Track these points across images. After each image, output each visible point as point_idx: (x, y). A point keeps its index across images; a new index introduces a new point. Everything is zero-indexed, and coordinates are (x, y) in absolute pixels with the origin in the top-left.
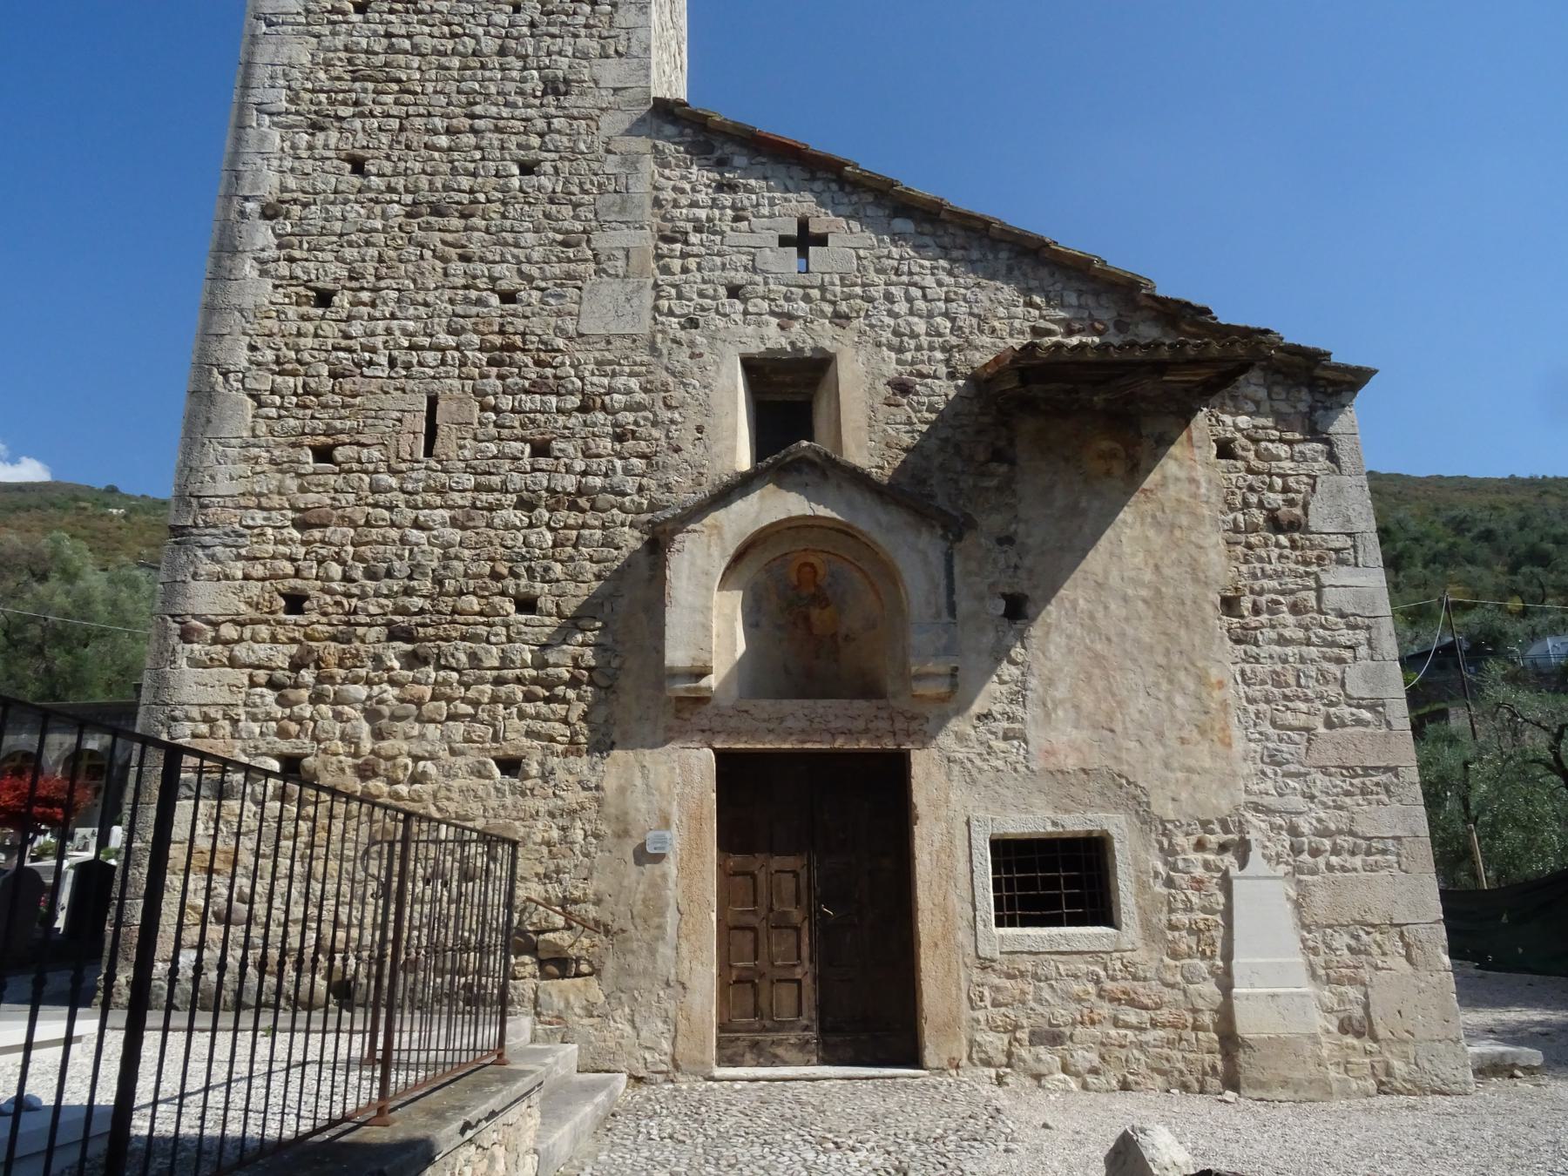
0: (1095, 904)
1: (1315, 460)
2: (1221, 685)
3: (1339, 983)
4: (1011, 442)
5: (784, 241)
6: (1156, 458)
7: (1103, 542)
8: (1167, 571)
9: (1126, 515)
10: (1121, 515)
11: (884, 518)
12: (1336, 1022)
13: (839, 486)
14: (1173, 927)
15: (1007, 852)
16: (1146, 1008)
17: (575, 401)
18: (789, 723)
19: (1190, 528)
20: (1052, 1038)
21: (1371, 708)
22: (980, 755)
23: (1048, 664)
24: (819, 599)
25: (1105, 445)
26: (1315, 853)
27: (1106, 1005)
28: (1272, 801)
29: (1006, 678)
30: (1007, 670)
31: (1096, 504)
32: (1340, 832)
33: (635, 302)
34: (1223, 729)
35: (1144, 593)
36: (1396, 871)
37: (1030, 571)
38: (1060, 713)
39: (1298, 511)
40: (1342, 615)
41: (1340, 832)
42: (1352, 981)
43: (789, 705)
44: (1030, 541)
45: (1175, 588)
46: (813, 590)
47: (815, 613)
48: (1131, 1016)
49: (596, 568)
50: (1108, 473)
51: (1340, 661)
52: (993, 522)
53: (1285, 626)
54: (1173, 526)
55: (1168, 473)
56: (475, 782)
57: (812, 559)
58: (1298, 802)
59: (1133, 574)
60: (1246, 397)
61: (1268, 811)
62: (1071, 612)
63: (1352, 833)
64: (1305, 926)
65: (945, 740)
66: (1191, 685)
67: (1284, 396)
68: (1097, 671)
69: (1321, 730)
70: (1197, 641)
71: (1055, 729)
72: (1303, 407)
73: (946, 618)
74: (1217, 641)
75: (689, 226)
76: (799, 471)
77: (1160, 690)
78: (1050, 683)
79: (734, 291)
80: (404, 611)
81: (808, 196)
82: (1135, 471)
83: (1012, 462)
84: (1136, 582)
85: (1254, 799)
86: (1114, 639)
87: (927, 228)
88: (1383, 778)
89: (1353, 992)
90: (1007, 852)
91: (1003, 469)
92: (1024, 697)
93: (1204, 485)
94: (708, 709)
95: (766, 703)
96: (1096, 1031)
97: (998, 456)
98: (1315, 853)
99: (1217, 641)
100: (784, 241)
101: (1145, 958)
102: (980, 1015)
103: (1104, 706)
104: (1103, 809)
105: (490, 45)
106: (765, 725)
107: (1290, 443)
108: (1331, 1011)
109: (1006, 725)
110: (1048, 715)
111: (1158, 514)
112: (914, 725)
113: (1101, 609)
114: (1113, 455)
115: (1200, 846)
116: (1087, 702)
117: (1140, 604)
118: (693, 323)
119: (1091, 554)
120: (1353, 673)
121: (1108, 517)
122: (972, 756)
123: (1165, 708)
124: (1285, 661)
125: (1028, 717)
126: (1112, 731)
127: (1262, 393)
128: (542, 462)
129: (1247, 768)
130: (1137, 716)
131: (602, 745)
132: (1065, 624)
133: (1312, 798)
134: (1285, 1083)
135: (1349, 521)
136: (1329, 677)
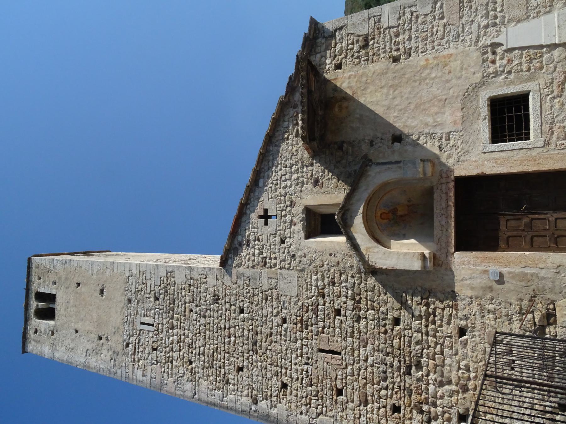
0: (520, 101)
2: (427, 60)
4: (336, 143)
5: (266, 224)
6: (341, 91)
7: (372, 108)
8: (383, 84)
9: (362, 100)
10: (362, 102)
11: (364, 188)
13: (352, 204)
14: (529, 70)
15: (496, 137)
17: (320, 299)
18: (443, 223)
19: (367, 76)
22: (456, 149)
23: (419, 125)
24: (394, 211)
25: (337, 109)
26: (496, 17)
28: (474, 36)
29: (425, 141)
30: (422, 141)
31: (358, 111)
32: (487, 9)
33: (286, 276)
34: (445, 58)
35: (391, 92)
37: (383, 134)
38: (439, 120)
39: (361, 38)
40: (400, 18)
41: (487, 9)
43: (436, 223)
44: (372, 134)
45: (389, 80)
46: (390, 214)
47: (399, 213)
49: (382, 295)
50: (347, 108)
51: (417, 17)
52: (365, 148)
53: (404, 38)
54: (366, 83)
55: (347, 86)
56: (469, 346)
57: (379, 215)
58: (474, 26)
59: (384, 96)
60: (320, 61)
61: (478, 37)
62: (399, 118)
63: (487, 4)
64: (528, 18)
65: (450, 163)
66: (428, 71)
67: (319, 48)
68: (422, 107)
69: (445, 21)
70: (409, 70)
71: (445, 121)
72: (323, 41)
73: (401, 165)
74: (410, 63)
75: (261, 256)
76: (346, 219)
77: (429, 83)
78: (427, 124)
79: (283, 241)
80: (399, 368)
81: (251, 215)
82: (345, 98)
83: (343, 142)
84: (387, 95)
86: (409, 101)
87: (262, 175)
90: (496, 137)
91: (345, 145)
92: (432, 134)
93: (351, 73)
94: (438, 254)
95: (435, 232)
97: (340, 148)
98: (496, 17)
99: (410, 63)
100: (266, 224)
103: (436, 103)
104: (478, 101)
105: (203, 321)
106: (444, 232)
107: (336, 44)
110: (439, 124)
111: (362, 88)
112: (444, 175)
113: (397, 107)
114: (340, 106)
115: (493, 62)
116: (434, 110)
117: (395, 93)
118: (293, 256)
119: (376, 112)
120: (422, 11)
121: (363, 107)
122: (457, 153)
123: (436, 80)
124: (418, 37)
125: (440, 132)
126: (446, 100)
127: (319, 55)
128: (342, 312)
129: (461, 47)
130: (440, 91)
131: (453, 296)
132: (403, 120)
133: (472, 21)
135: (364, 20)
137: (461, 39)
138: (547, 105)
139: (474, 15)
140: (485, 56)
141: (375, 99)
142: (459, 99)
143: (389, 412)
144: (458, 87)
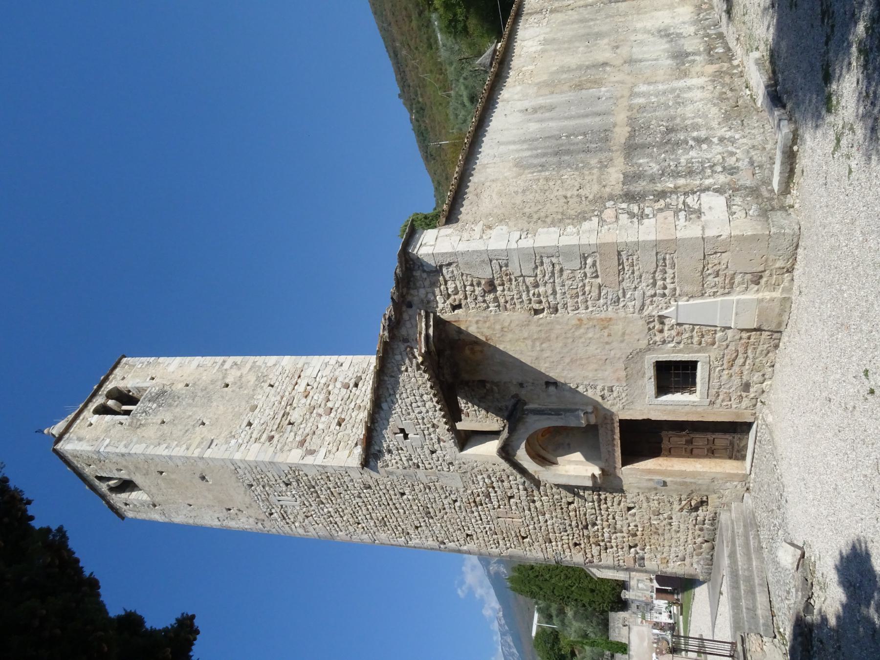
1: (452, 272)
3: (732, 284)
4: (474, 381)
6: (469, 334)
8: (526, 335)
12: (753, 285)
14: (700, 343)
16: (737, 356)
20: (746, 387)
21: (585, 259)
25: (467, 352)
26: (665, 288)
27: (734, 368)
28: (638, 304)
30: (581, 389)
32: (654, 277)
36: (675, 255)
39: (483, 282)
40: (536, 267)
41: (654, 277)
42: (733, 277)
48: (740, 361)
50: (482, 352)
51: (561, 270)
56: (637, 518)
61: (643, 305)
63: (655, 272)
64: (703, 295)
65: (614, 409)
69: (599, 280)
72: (425, 275)
80: (577, 526)
81: (384, 432)
84: (533, 347)
85: (637, 311)
88: (624, 257)
89: (738, 279)
96: (745, 373)
98: (665, 288)
101: (714, 352)
102: (734, 406)
104: (643, 362)
107: (446, 282)
108: (747, 288)
109: (606, 391)
114: (472, 350)
115: (661, 331)
116: (595, 366)
124: (565, 293)
129: (622, 313)
130: (599, 351)
131: (622, 491)
133: (636, 288)
134: (780, 315)
136: (571, 275)
137: (622, 304)
139: (636, 282)
140: (651, 326)
141: (518, 348)
142: (621, 361)
143: (572, 547)
144: (620, 350)
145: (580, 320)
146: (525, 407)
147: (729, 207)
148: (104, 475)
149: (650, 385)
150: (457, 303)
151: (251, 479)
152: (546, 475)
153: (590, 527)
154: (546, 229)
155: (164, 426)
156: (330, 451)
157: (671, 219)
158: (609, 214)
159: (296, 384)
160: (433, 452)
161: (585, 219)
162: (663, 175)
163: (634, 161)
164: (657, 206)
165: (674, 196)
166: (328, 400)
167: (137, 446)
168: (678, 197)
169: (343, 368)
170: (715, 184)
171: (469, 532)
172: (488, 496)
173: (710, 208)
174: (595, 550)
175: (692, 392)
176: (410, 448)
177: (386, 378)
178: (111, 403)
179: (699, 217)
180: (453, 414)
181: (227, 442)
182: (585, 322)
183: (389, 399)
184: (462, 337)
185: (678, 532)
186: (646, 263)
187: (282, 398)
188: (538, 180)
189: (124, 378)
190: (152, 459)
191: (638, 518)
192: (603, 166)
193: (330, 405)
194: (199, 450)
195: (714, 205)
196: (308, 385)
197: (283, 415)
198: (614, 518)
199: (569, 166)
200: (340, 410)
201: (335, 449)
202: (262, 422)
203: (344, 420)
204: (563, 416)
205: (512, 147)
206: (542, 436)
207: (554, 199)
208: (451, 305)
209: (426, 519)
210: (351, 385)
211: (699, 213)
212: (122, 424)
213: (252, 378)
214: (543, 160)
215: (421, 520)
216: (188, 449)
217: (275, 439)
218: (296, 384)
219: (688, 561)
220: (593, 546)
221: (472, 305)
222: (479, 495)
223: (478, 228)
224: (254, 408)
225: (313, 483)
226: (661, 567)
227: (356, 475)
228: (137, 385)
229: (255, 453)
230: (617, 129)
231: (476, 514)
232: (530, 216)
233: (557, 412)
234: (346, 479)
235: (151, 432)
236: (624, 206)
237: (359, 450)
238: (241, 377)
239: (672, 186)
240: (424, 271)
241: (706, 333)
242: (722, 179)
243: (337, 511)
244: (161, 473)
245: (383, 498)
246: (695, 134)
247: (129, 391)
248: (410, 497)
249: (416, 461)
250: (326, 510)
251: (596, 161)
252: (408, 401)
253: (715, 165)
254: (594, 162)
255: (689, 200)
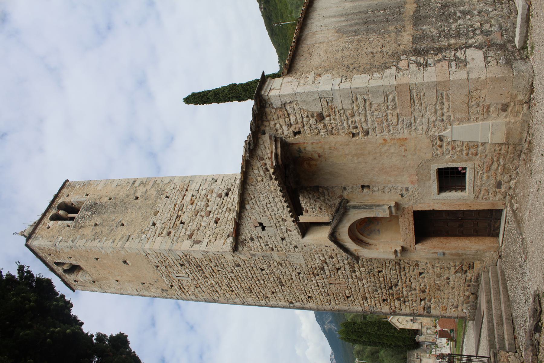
3: (488, 111)
4: (310, 187)
14: (467, 154)
16: (492, 163)
20: (499, 185)
25: (306, 166)
40: (353, 102)
48: (495, 166)
53: (360, 120)
56: (426, 279)
58: (425, 120)
79: (283, 239)
80: (385, 288)
85: (424, 132)
96: (499, 175)
101: (477, 161)
102: (491, 199)
104: (429, 169)
108: (498, 115)
115: (441, 146)
124: (374, 121)
129: (414, 134)
134: (521, 133)
138: (478, 177)
143: (381, 302)
145: (385, 140)
146: (348, 204)
147: (485, 58)
148: (60, 261)
149: (434, 186)
150: (297, 130)
151: (157, 262)
152: (364, 252)
153: (393, 287)
154: (359, 76)
155: (97, 227)
156: (210, 241)
157: (446, 67)
158: (403, 64)
159: (185, 195)
160: (283, 239)
161: (386, 68)
162: (440, 36)
163: (420, 27)
164: (436, 58)
165: (448, 51)
166: (208, 206)
167: (80, 241)
168: (450, 52)
169: (217, 183)
170: (476, 42)
171: (310, 295)
172: (323, 269)
173: (473, 59)
174: (397, 303)
175: (463, 188)
176: (267, 237)
177: (248, 187)
178: (61, 212)
179: (465, 65)
180: (296, 210)
181: (140, 237)
182: (388, 141)
183: (250, 202)
184: (302, 155)
185: (453, 288)
186: (430, 97)
187: (175, 205)
188: (353, 41)
189: (68, 195)
190: (90, 250)
191: (427, 281)
192: (398, 32)
193: (209, 209)
194: (121, 242)
195: (475, 56)
196: (193, 196)
197: (177, 217)
198: (410, 281)
199: (374, 31)
200: (216, 213)
201: (214, 239)
202: (162, 222)
203: (219, 219)
204: (374, 210)
205: (334, 20)
206: (360, 225)
207: (365, 55)
208: (293, 132)
209: (280, 286)
210: (224, 195)
211: (465, 62)
212: (69, 226)
213: (154, 192)
214: (356, 28)
215: (276, 288)
216: (113, 242)
217: (172, 234)
218: (185, 195)
219: (460, 308)
220: (396, 301)
221: (308, 132)
222: (316, 269)
223: (311, 76)
224: (156, 213)
225: (200, 264)
226: (442, 313)
227: (229, 257)
228: (78, 200)
229: (159, 244)
230: (407, 6)
231: (314, 282)
232: (348, 67)
233: (371, 207)
234: (223, 260)
235: (88, 231)
236: (413, 58)
237: (231, 239)
238: (146, 192)
239: (447, 44)
240: (273, 108)
241: (472, 148)
242: (480, 39)
243: (217, 283)
244: (97, 259)
245: (249, 273)
246: (462, 8)
247: (73, 204)
248: (268, 272)
249: (271, 246)
250: (209, 283)
251: (393, 28)
252: (264, 203)
253: (475, 29)
254: (391, 28)
255: (458, 54)
